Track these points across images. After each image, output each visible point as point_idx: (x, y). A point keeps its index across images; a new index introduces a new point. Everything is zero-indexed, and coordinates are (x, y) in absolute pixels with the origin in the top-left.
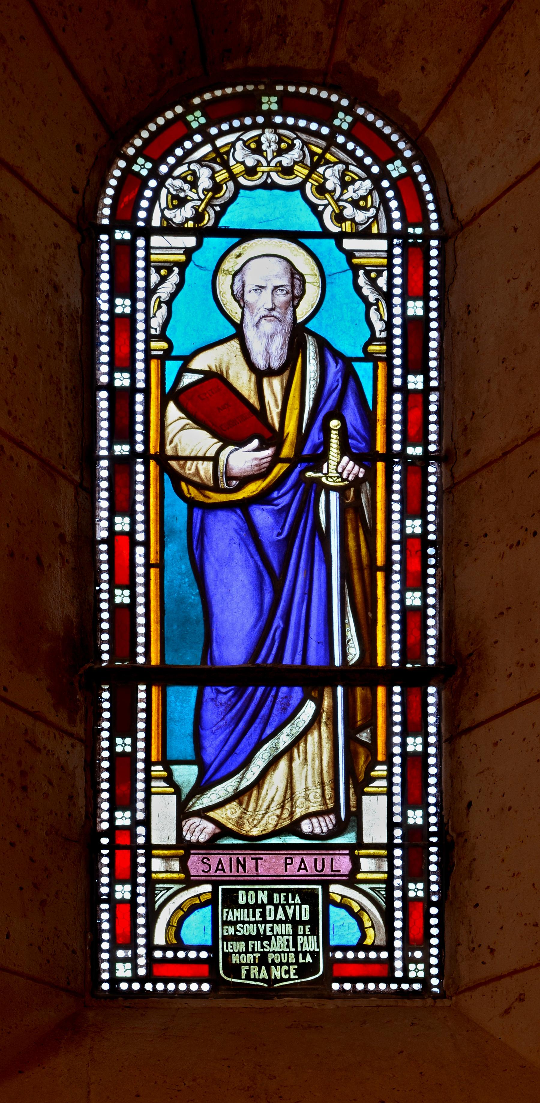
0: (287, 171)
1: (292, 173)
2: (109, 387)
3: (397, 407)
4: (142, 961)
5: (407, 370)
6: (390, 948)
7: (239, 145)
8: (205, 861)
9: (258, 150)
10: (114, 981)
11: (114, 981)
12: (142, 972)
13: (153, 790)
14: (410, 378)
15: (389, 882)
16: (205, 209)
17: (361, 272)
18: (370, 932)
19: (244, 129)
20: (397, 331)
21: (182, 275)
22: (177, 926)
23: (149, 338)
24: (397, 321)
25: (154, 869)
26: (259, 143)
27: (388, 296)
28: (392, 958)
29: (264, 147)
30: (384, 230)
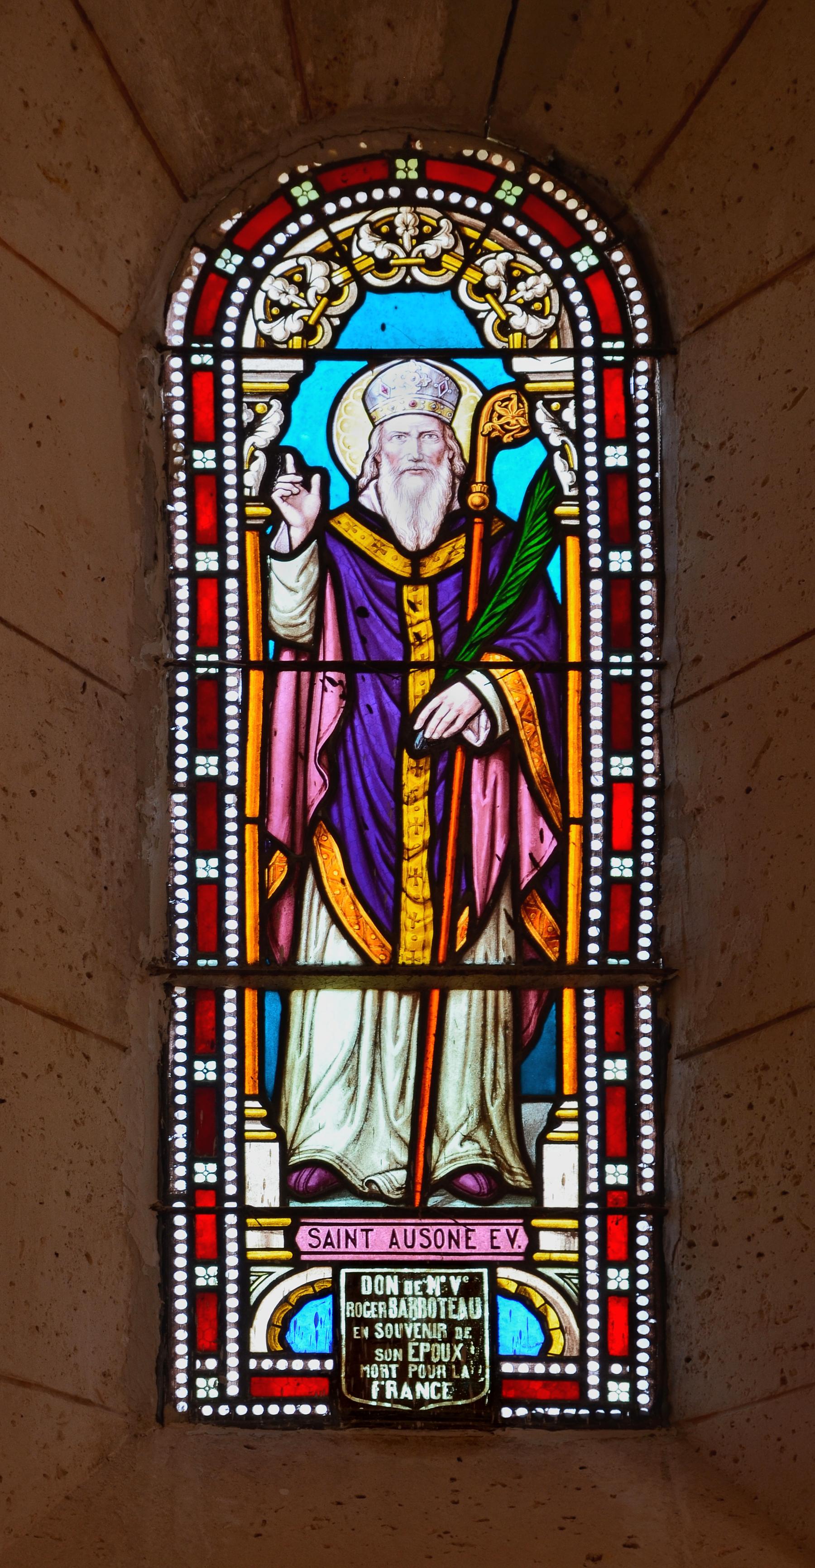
0: (433, 264)
1: (440, 267)
2: (190, 572)
3: (596, 599)
4: (233, 1376)
5: (609, 543)
6: (582, 1360)
7: (365, 230)
8: (313, 1233)
9: (392, 237)
10: (194, 1402)
11: (194, 1402)
12: (233, 1390)
13: (247, 1135)
14: (613, 555)
15: (581, 1265)
16: (318, 322)
17: (539, 404)
18: (557, 1336)
19: (373, 205)
20: (592, 491)
21: (287, 410)
22: (282, 1324)
23: (242, 501)
24: (592, 476)
25: (249, 1245)
26: (392, 226)
27: (578, 438)
28: (583, 1371)
29: (399, 231)
30: (569, 344)
